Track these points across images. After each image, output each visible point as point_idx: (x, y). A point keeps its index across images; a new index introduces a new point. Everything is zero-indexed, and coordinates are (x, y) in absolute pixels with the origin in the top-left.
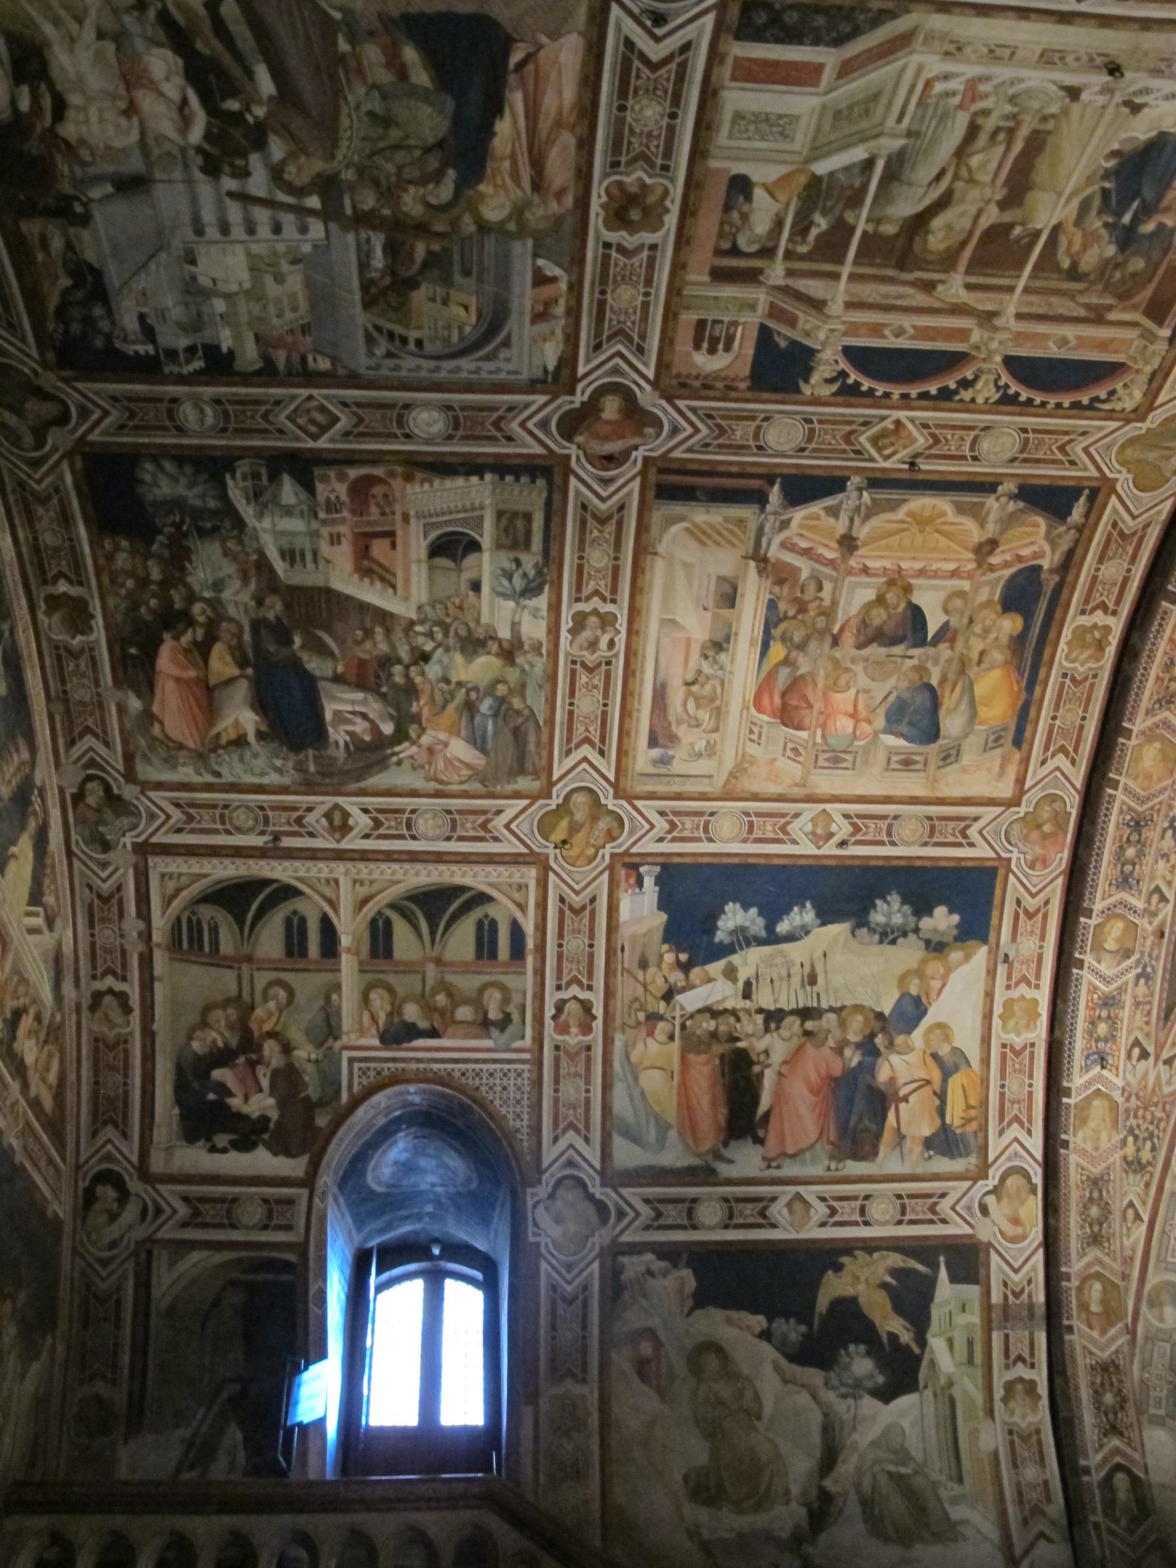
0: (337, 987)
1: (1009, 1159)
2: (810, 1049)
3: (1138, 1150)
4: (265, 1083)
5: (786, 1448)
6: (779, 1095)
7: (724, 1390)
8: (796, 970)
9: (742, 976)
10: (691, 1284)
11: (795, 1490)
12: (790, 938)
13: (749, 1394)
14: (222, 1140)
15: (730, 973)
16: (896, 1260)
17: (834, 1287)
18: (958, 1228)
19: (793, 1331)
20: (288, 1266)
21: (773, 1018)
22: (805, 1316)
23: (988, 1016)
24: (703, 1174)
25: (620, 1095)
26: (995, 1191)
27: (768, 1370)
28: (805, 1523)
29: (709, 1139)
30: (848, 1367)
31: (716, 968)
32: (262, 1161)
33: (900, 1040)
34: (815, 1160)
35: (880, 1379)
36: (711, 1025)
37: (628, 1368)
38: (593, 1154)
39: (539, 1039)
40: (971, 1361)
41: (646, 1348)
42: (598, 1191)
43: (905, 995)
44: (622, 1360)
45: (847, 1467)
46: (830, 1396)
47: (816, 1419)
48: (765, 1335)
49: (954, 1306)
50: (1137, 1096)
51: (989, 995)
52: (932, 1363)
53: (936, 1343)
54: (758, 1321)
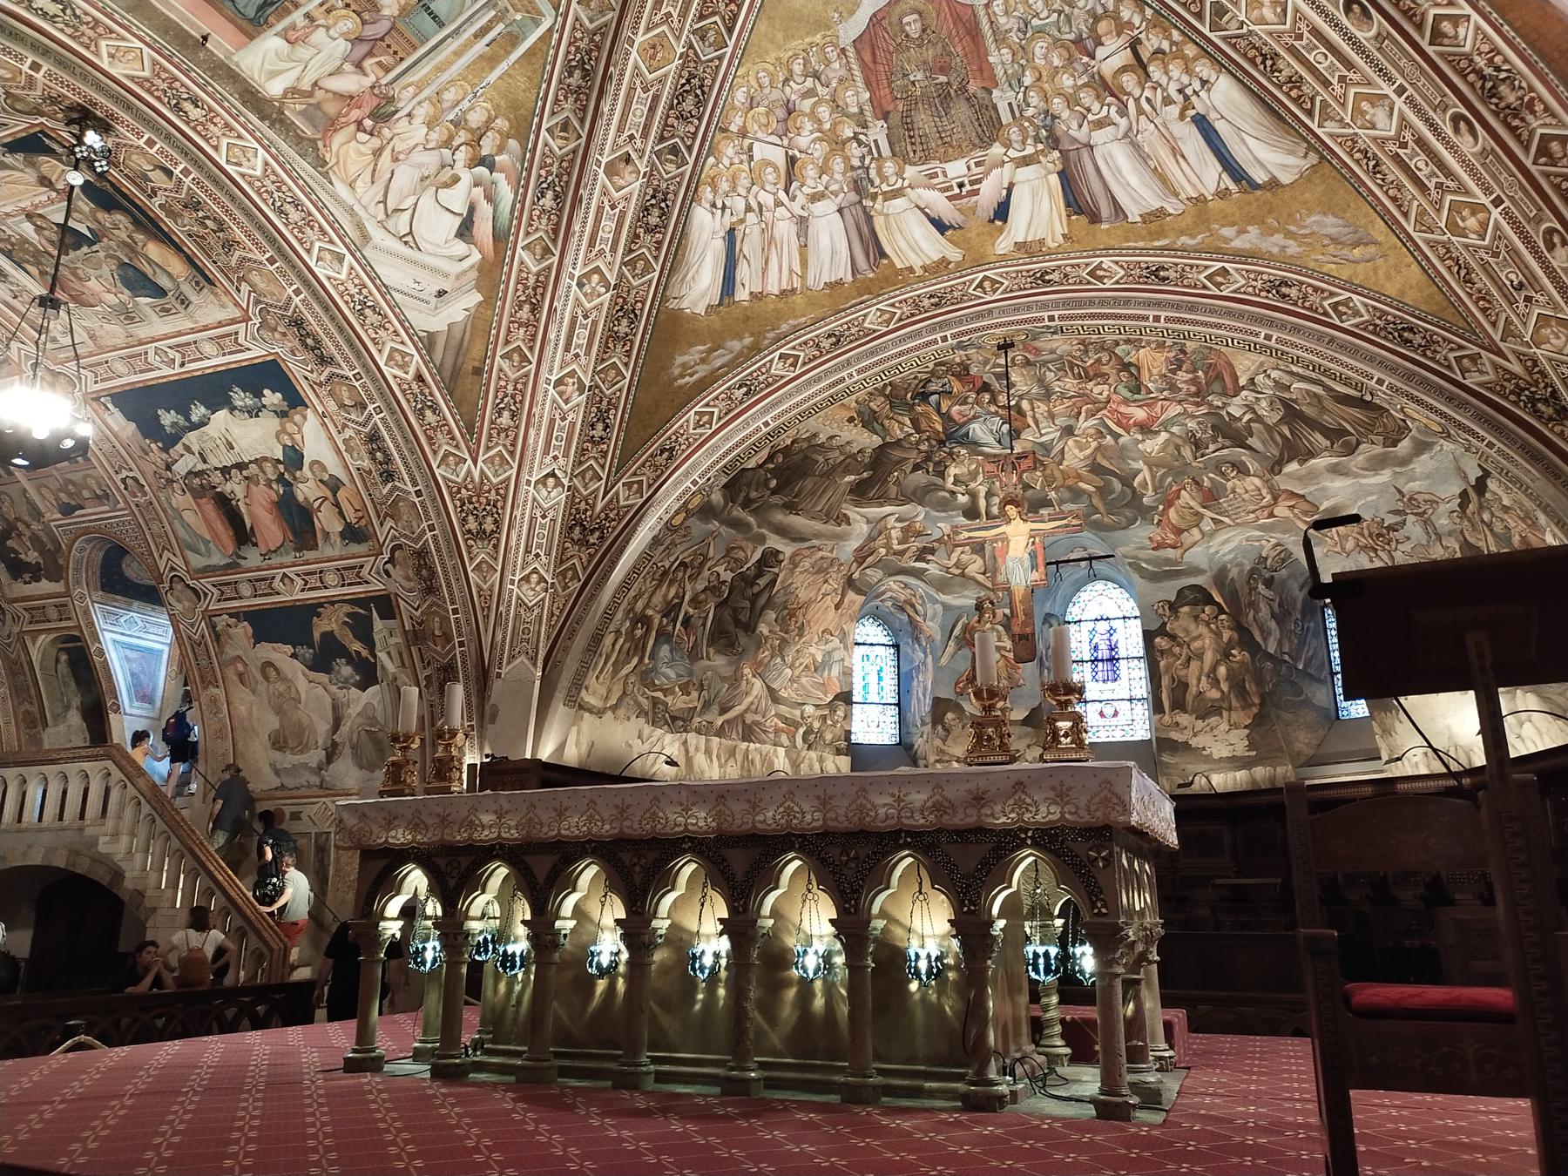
0: (25, 490)
1: (392, 541)
2: (253, 487)
3: (480, 524)
4: (29, 544)
5: (314, 717)
6: (252, 516)
7: (282, 688)
8: (218, 442)
9: (195, 448)
10: (250, 630)
11: (320, 742)
12: (203, 423)
13: (293, 689)
14: (27, 577)
15: (188, 449)
16: (347, 608)
17: (321, 626)
18: (376, 586)
19: (307, 653)
20: (77, 639)
21: (225, 471)
22: (311, 645)
23: (338, 451)
24: (232, 567)
25: (177, 526)
26: (391, 560)
27: (300, 674)
28: (324, 760)
29: (231, 549)
30: (339, 672)
31: (179, 447)
32: (45, 586)
33: (298, 474)
34: (288, 553)
35: (358, 678)
36: (197, 481)
37: (235, 678)
38: (179, 562)
39: (126, 502)
40: (403, 665)
41: (240, 667)
42: (190, 582)
43: (285, 446)
44: (231, 673)
45: (345, 729)
46: (334, 688)
47: (328, 700)
48: (294, 656)
49: (385, 633)
50: (466, 487)
51: (331, 438)
52: (383, 667)
53: (382, 656)
54: (289, 649)
